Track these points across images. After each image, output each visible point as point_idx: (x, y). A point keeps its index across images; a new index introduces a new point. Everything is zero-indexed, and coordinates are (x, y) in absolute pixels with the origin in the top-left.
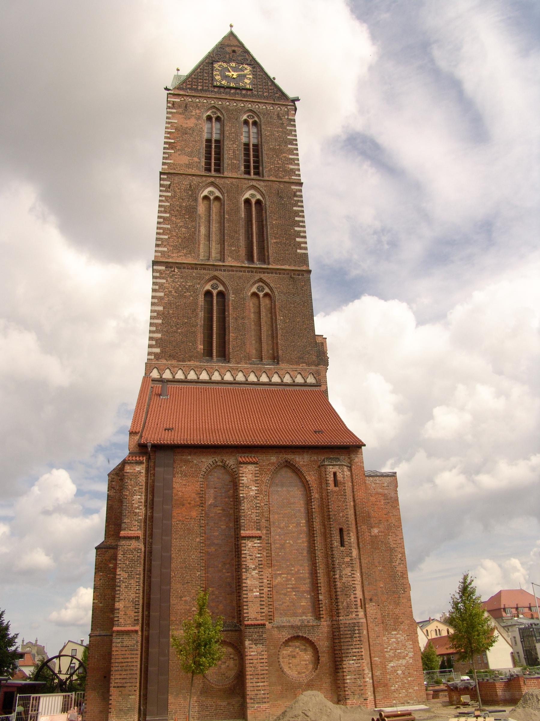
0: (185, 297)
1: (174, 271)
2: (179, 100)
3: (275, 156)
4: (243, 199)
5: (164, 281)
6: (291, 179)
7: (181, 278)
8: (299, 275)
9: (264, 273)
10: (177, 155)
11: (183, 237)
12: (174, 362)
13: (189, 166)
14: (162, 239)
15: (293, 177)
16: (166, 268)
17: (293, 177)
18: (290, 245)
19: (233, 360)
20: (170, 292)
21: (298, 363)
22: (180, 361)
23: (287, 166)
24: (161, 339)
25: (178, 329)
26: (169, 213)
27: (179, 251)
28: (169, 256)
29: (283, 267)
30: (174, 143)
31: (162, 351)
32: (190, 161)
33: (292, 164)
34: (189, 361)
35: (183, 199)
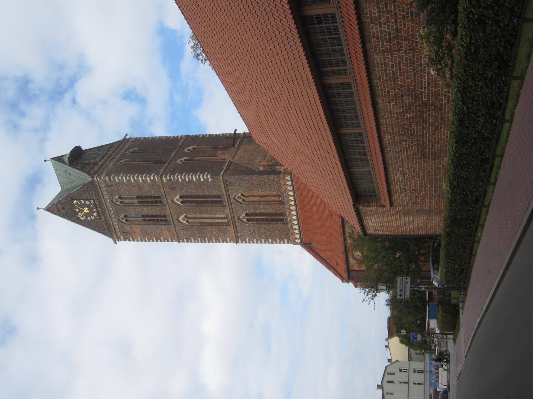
0: (254, 230)
2: (122, 237)
4: (182, 205)
7: (243, 232)
8: (226, 181)
9: (230, 197)
12: (290, 234)
15: (157, 180)
16: (239, 238)
17: (157, 180)
18: (208, 184)
19: (284, 211)
20: (252, 236)
21: (280, 184)
22: (289, 232)
23: (149, 184)
24: (279, 239)
25: (272, 233)
26: (205, 238)
27: (228, 233)
28: (231, 237)
29: (223, 188)
31: (286, 239)
32: (165, 230)
33: (147, 181)
34: (288, 228)
35: (194, 233)
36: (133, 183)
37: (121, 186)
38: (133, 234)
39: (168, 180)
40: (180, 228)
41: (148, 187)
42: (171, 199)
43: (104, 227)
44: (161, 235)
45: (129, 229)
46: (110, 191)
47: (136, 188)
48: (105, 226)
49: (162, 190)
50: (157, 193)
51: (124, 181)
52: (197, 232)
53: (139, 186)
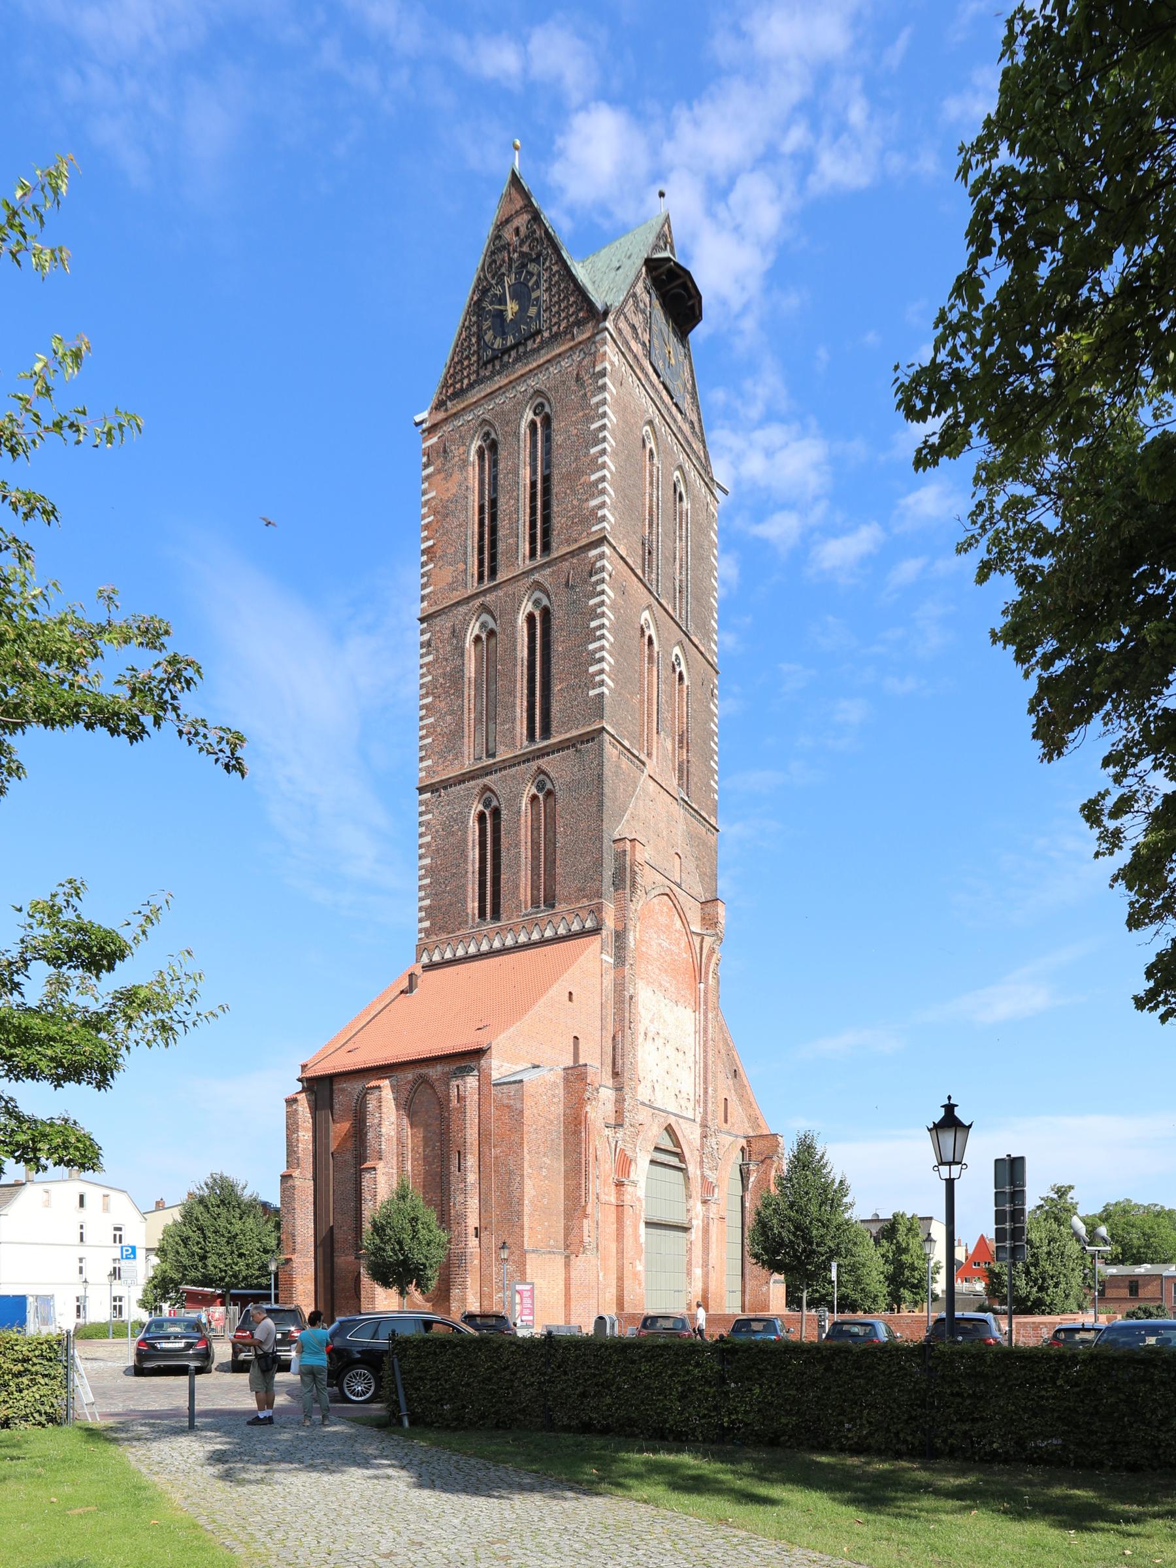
0: (453, 834)
1: (440, 796)
3: (568, 491)
5: (430, 816)
6: (592, 533)
10: (437, 570)
11: (448, 732)
13: (452, 587)
14: (425, 745)
15: (594, 529)
17: (594, 529)
20: (437, 831)
23: (585, 505)
30: (434, 544)
33: (593, 496)
35: (447, 660)
36: (587, 454)
37: (581, 414)
38: (443, 475)
39: (594, 564)
40: (460, 617)
41: (575, 503)
42: (541, 580)
43: (461, 381)
44: (440, 564)
45: (457, 459)
46: (564, 383)
47: (574, 465)
48: (466, 382)
49: (565, 549)
50: (558, 534)
51: (592, 423)
52: (448, 669)
53: (580, 472)
